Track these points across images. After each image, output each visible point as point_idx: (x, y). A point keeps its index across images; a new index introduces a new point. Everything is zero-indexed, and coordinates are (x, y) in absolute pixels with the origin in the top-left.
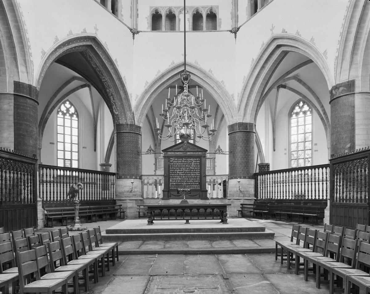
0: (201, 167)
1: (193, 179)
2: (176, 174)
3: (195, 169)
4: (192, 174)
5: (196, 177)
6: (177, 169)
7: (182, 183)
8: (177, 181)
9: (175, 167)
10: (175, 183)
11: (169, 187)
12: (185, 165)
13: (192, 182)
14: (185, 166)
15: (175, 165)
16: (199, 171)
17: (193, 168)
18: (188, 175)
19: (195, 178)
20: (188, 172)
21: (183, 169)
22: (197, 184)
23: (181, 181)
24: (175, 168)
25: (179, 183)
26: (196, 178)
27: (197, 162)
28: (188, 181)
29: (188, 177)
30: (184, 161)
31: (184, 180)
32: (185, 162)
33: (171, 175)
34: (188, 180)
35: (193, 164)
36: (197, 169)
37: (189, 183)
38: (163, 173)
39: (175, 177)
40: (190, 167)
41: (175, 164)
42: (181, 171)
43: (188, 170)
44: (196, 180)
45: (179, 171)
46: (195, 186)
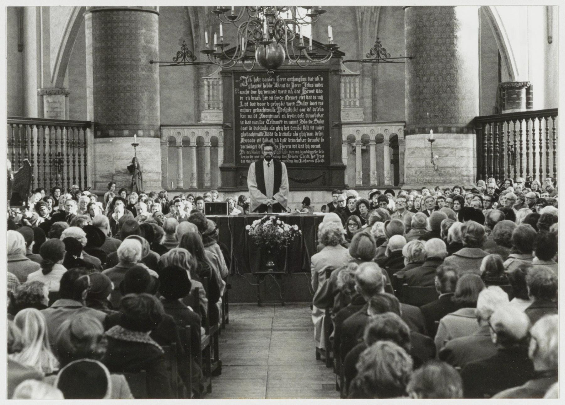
0: (326, 100)
1: (304, 134)
2: (257, 119)
3: (309, 106)
5: (312, 128)
9: (253, 101)
10: (254, 147)
12: (283, 95)
14: (281, 98)
15: (254, 95)
16: (321, 113)
18: (291, 122)
19: (310, 131)
20: (290, 113)
21: (276, 107)
22: (317, 149)
24: (254, 104)
26: (313, 131)
27: (316, 85)
28: (290, 140)
29: (292, 128)
30: (281, 83)
31: (278, 137)
32: (283, 86)
33: (242, 123)
35: (304, 92)
37: (294, 147)
39: (255, 128)
40: (295, 101)
41: (255, 92)
43: (290, 110)
44: (314, 137)
45: (266, 113)
46: (312, 152)
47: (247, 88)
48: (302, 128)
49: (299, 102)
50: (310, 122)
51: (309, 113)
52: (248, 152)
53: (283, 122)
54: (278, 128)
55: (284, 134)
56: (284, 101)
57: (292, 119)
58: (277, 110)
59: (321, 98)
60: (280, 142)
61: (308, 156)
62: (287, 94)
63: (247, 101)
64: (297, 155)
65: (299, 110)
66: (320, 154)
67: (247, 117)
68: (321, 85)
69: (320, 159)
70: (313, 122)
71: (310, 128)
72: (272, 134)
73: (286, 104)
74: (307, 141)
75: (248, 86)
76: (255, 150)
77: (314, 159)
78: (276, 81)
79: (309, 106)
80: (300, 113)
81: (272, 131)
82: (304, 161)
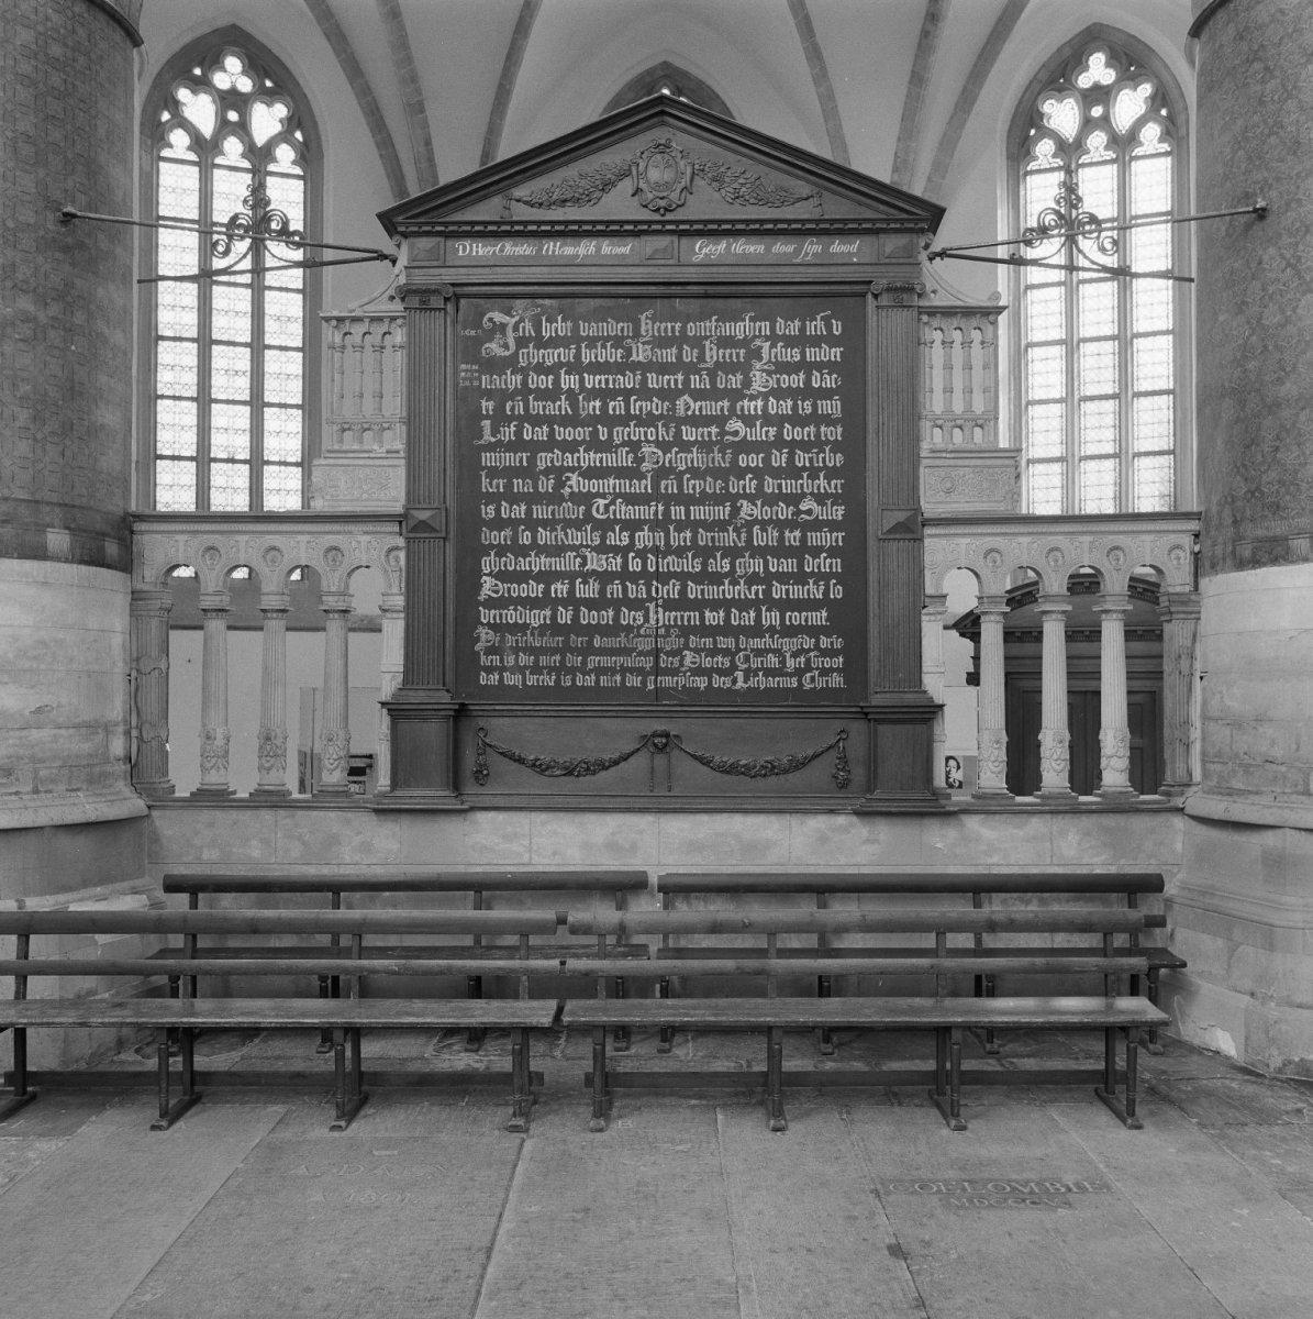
0: (854, 419)
1: (756, 565)
2: (555, 498)
3: (779, 442)
5: (792, 537)
6: (571, 447)
7: (628, 617)
8: (560, 588)
9: (537, 421)
10: (537, 618)
11: (467, 664)
12: (668, 395)
13: (743, 605)
14: (657, 407)
15: (543, 395)
16: (832, 473)
17: (762, 433)
18: (698, 512)
19: (781, 551)
20: (695, 473)
21: (634, 447)
22: (814, 631)
23: (615, 589)
24: (542, 433)
25: (588, 617)
27: (812, 354)
28: (694, 592)
29: (704, 538)
30: (661, 342)
32: (670, 355)
33: (489, 512)
34: (700, 578)
35: (759, 382)
36: (805, 446)
37: (713, 618)
38: (391, 493)
39: (544, 536)
40: (720, 421)
41: (546, 382)
42: (620, 472)
43: (696, 458)
44: (801, 578)
46: (788, 645)
47: (511, 363)
49: (735, 425)
50: (784, 511)
51: (777, 473)
52: (510, 640)
53: (667, 512)
54: (644, 538)
55: (671, 563)
56: (670, 419)
57: (704, 498)
58: (639, 460)
59: (832, 407)
60: (650, 599)
61: (772, 661)
62: (687, 389)
64: (726, 652)
65: (735, 461)
66: (825, 653)
67: (509, 486)
68: (835, 353)
69: (825, 672)
70: (798, 512)
71: (781, 538)
72: (616, 563)
73: (678, 433)
74: (767, 592)
77: (799, 673)
78: (637, 335)
79: (779, 442)
80: (741, 473)
81: (616, 550)
82: (752, 683)
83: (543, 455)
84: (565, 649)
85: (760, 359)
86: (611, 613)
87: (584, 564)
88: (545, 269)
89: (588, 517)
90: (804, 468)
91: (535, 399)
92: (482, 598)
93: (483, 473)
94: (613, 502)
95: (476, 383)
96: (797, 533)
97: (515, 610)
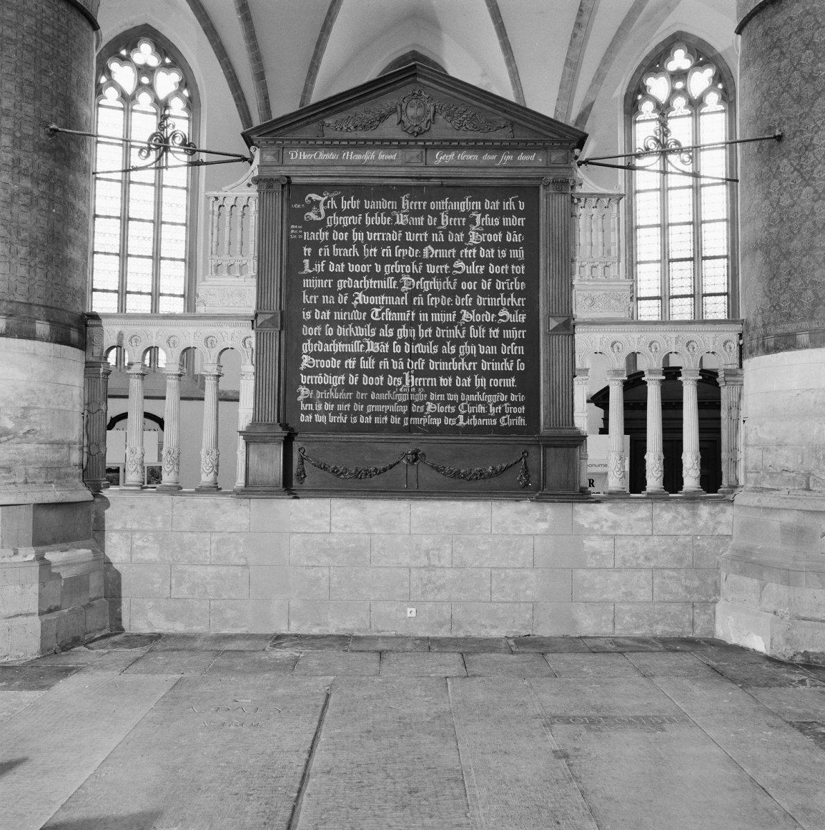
1: (472, 350)
2: (348, 307)
3: (486, 275)
4: (466, 315)
5: (494, 333)
6: (358, 276)
7: (392, 381)
8: (351, 363)
9: (338, 260)
10: (337, 380)
12: (419, 245)
13: (464, 374)
14: (412, 252)
15: (341, 244)
16: (518, 294)
17: (474, 269)
18: (436, 317)
19: (487, 341)
21: (397, 276)
22: (507, 391)
23: (384, 364)
24: (341, 268)
25: (367, 381)
26: (498, 342)
27: (507, 221)
28: (433, 365)
29: (440, 333)
30: (414, 213)
31: (402, 356)
32: (420, 221)
33: (307, 315)
34: (438, 357)
35: (474, 238)
36: (502, 277)
37: (445, 382)
39: (341, 331)
40: (450, 261)
41: (343, 236)
42: (388, 292)
43: (436, 284)
44: (499, 358)
45: (370, 292)
46: (491, 399)
48: (468, 333)
49: (459, 264)
50: (489, 317)
51: (485, 294)
52: (319, 394)
53: (417, 317)
54: (403, 332)
55: (420, 348)
56: (419, 260)
57: (440, 309)
58: (400, 285)
59: (518, 254)
60: (406, 370)
61: (481, 409)
62: (430, 242)
63: (323, 258)
64: (453, 403)
65: (459, 285)
66: (514, 404)
67: (320, 300)
68: (520, 221)
69: (513, 416)
70: (497, 318)
71: (487, 334)
72: (385, 348)
73: (424, 268)
74: (479, 366)
75: (325, 220)
76: (339, 388)
77: (498, 416)
78: (399, 208)
79: (486, 275)
80: (462, 293)
81: (385, 339)
82: (468, 422)
83: (341, 281)
84: (353, 400)
85: (475, 224)
86: (382, 378)
87: (365, 348)
88: (344, 168)
89: (368, 319)
90: (501, 291)
91: (336, 247)
92: (302, 368)
93: (304, 292)
94: (384, 310)
95: (300, 237)
96: (497, 331)
97: (323, 376)
